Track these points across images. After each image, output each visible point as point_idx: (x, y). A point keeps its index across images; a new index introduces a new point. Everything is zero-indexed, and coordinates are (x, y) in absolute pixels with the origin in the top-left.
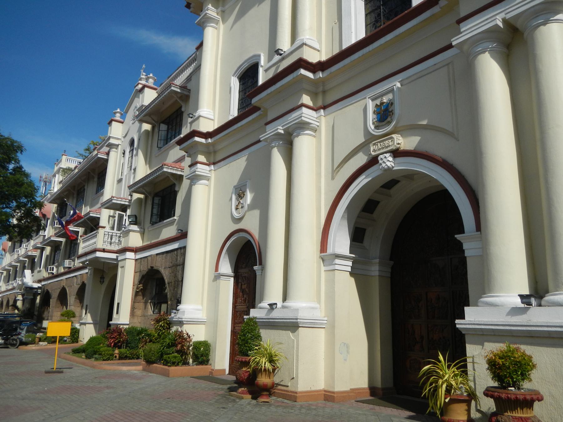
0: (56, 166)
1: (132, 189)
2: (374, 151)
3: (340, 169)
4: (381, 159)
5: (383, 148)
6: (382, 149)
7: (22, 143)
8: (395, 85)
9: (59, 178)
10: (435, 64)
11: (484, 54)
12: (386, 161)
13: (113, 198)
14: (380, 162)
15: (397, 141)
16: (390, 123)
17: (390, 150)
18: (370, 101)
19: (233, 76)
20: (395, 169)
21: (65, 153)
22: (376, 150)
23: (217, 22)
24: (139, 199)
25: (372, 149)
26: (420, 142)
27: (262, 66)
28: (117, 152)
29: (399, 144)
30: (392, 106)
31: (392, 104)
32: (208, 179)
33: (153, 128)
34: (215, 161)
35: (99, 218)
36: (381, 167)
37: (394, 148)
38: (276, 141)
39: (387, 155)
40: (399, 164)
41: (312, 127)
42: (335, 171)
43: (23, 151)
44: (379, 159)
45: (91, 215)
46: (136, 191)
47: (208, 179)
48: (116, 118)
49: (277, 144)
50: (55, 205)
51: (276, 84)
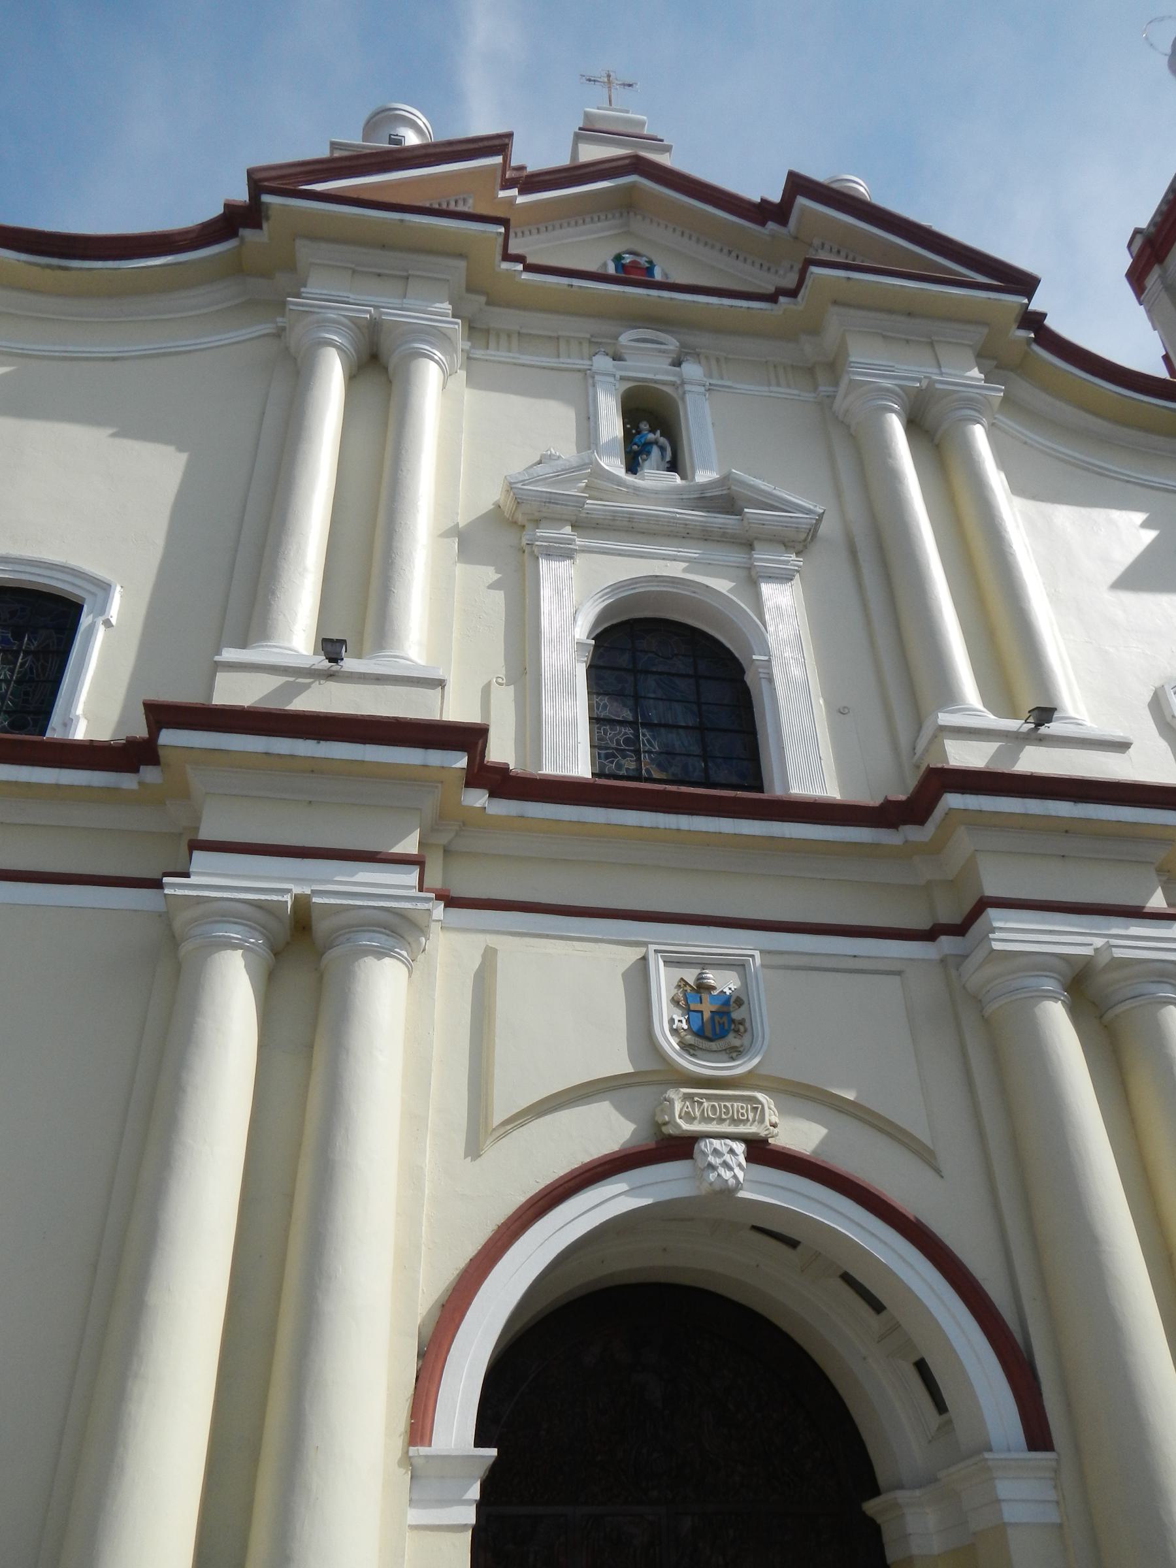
2: (689, 1118)
4: (716, 1152)
5: (721, 1120)
6: (718, 1124)
8: (752, 956)
10: (855, 956)
11: (1056, 1003)
12: (733, 1164)
15: (770, 1115)
16: (734, 1053)
17: (749, 1133)
18: (661, 963)
20: (742, 1194)
22: (695, 1118)
25: (678, 1106)
26: (824, 1142)
27: (108, 623)
29: (774, 1126)
30: (739, 1007)
36: (712, 1176)
38: (247, 928)
40: (758, 1184)
41: (420, 943)
42: (494, 1129)
44: (707, 1146)
49: (252, 940)
51: (322, 743)
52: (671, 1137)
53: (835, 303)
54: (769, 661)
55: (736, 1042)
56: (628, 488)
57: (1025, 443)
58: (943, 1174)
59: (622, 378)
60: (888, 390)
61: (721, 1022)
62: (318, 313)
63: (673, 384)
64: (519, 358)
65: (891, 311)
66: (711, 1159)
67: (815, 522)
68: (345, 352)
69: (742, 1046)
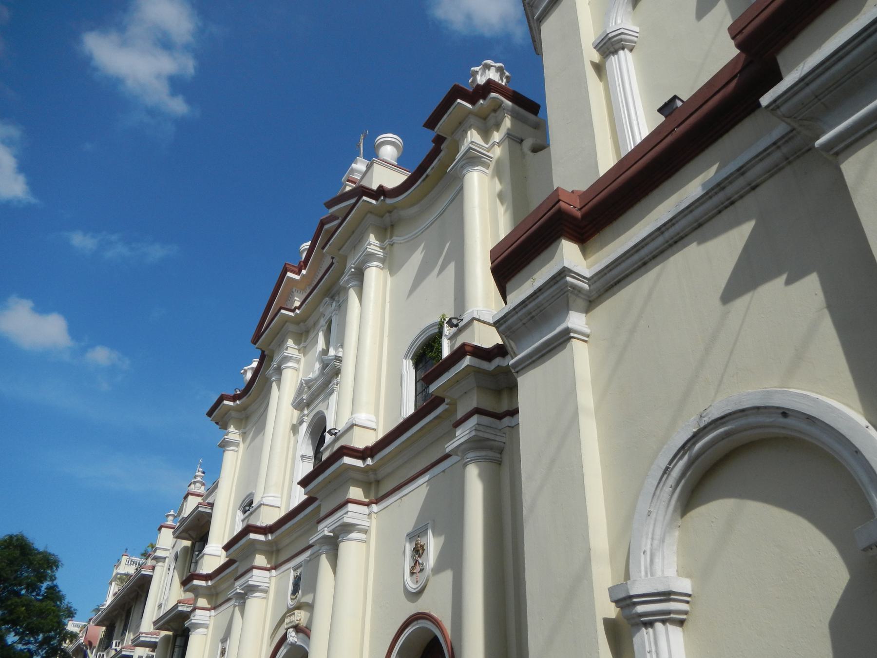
0: (115, 569)
1: (158, 625)
3: (275, 636)
7: (59, 557)
9: (114, 588)
13: (141, 635)
16: (297, 596)
18: (292, 571)
19: (239, 509)
20: (297, 644)
21: (126, 552)
23: (237, 445)
24: (166, 637)
28: (163, 567)
29: (297, 620)
32: (206, 626)
33: (193, 545)
34: (218, 604)
35: (132, 656)
39: (291, 630)
41: (260, 589)
43: (60, 567)
45: (124, 653)
46: (161, 628)
47: (206, 626)
48: (167, 523)
50: (104, 628)
53: (339, 250)
56: (314, 380)
59: (326, 323)
60: (347, 280)
65: (350, 236)
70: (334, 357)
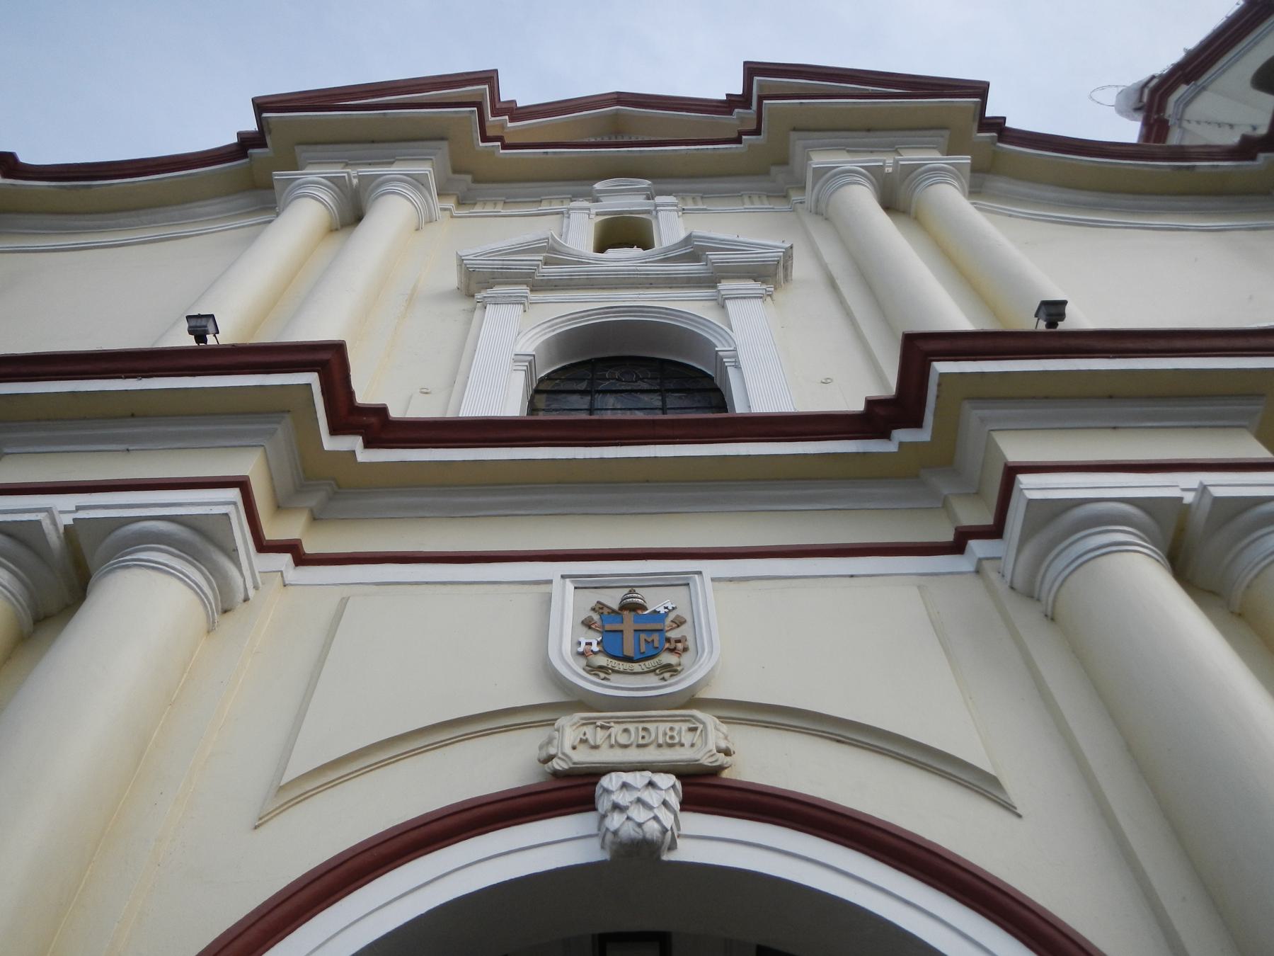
10: (852, 576)
14: (603, 804)
31: (679, 623)
37: (706, 761)
44: (610, 781)
52: (556, 774)
53: (795, 129)
54: (735, 350)
55: (670, 659)
57: (1010, 216)
58: (1018, 811)
59: (597, 214)
61: (650, 640)
62: (299, 178)
63: (648, 212)
64: (500, 212)
66: (623, 798)
67: (782, 254)
68: (325, 206)
69: (680, 665)
70: (788, 245)
